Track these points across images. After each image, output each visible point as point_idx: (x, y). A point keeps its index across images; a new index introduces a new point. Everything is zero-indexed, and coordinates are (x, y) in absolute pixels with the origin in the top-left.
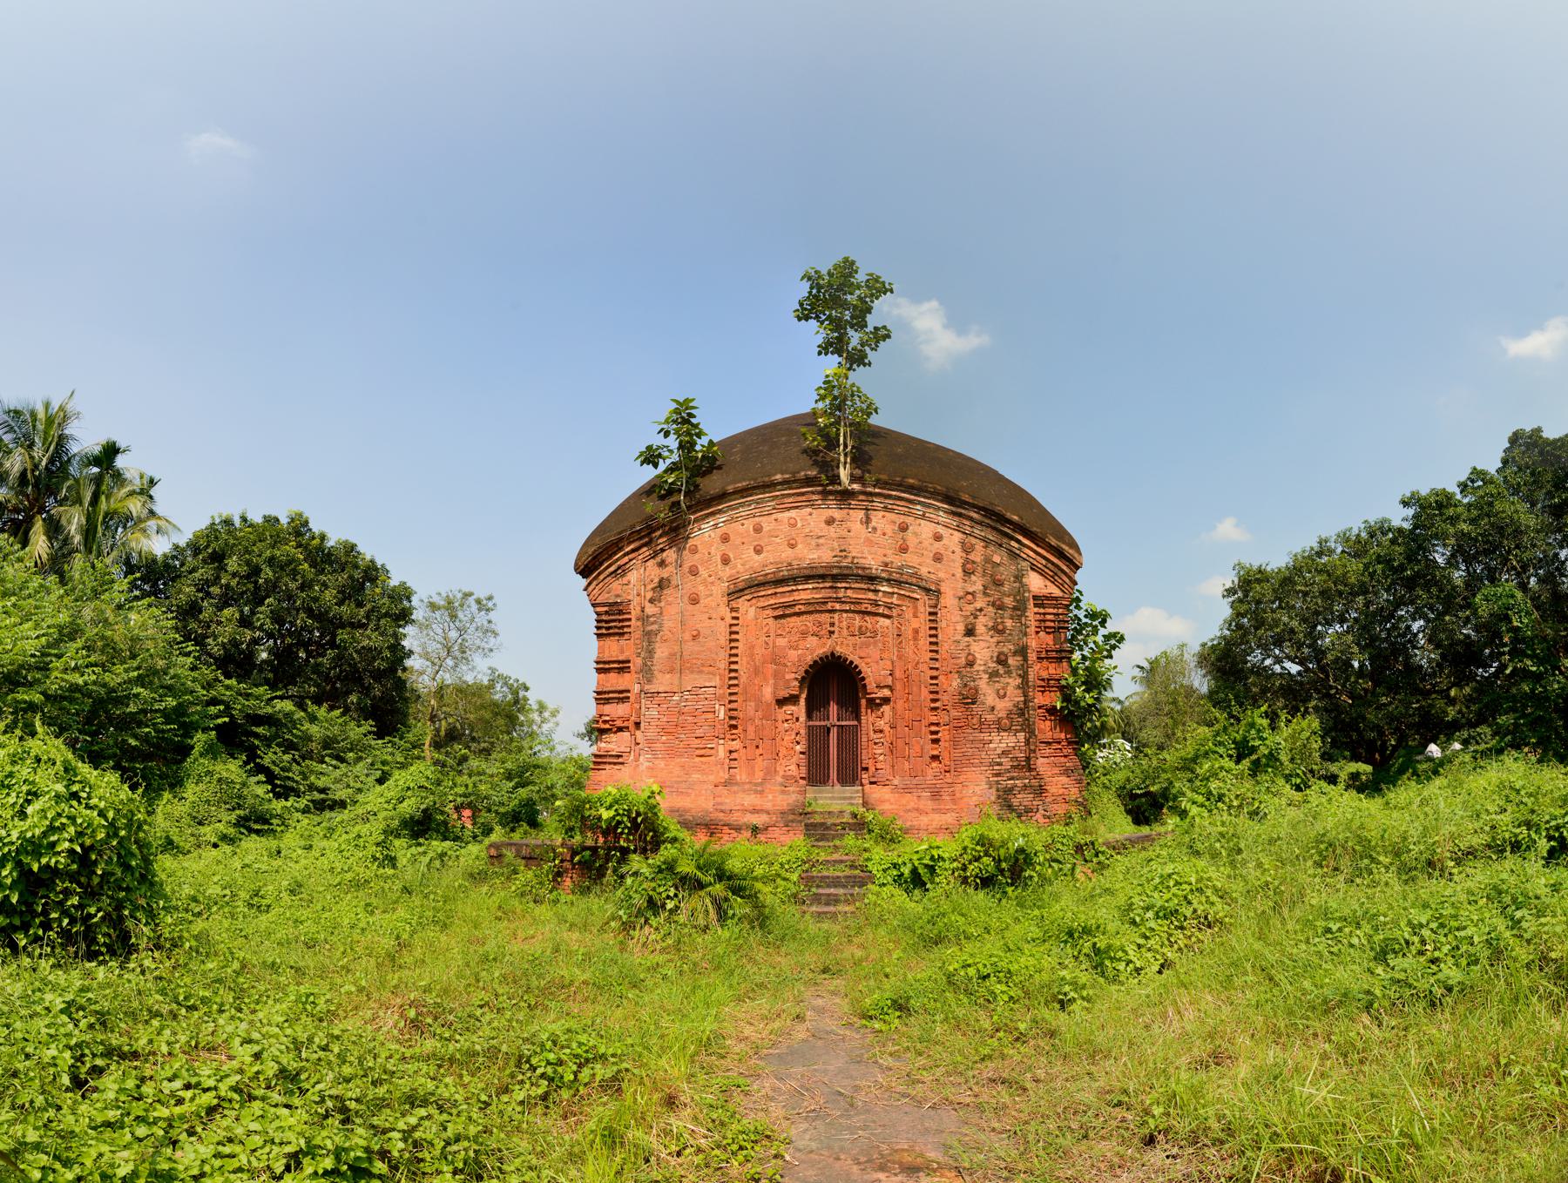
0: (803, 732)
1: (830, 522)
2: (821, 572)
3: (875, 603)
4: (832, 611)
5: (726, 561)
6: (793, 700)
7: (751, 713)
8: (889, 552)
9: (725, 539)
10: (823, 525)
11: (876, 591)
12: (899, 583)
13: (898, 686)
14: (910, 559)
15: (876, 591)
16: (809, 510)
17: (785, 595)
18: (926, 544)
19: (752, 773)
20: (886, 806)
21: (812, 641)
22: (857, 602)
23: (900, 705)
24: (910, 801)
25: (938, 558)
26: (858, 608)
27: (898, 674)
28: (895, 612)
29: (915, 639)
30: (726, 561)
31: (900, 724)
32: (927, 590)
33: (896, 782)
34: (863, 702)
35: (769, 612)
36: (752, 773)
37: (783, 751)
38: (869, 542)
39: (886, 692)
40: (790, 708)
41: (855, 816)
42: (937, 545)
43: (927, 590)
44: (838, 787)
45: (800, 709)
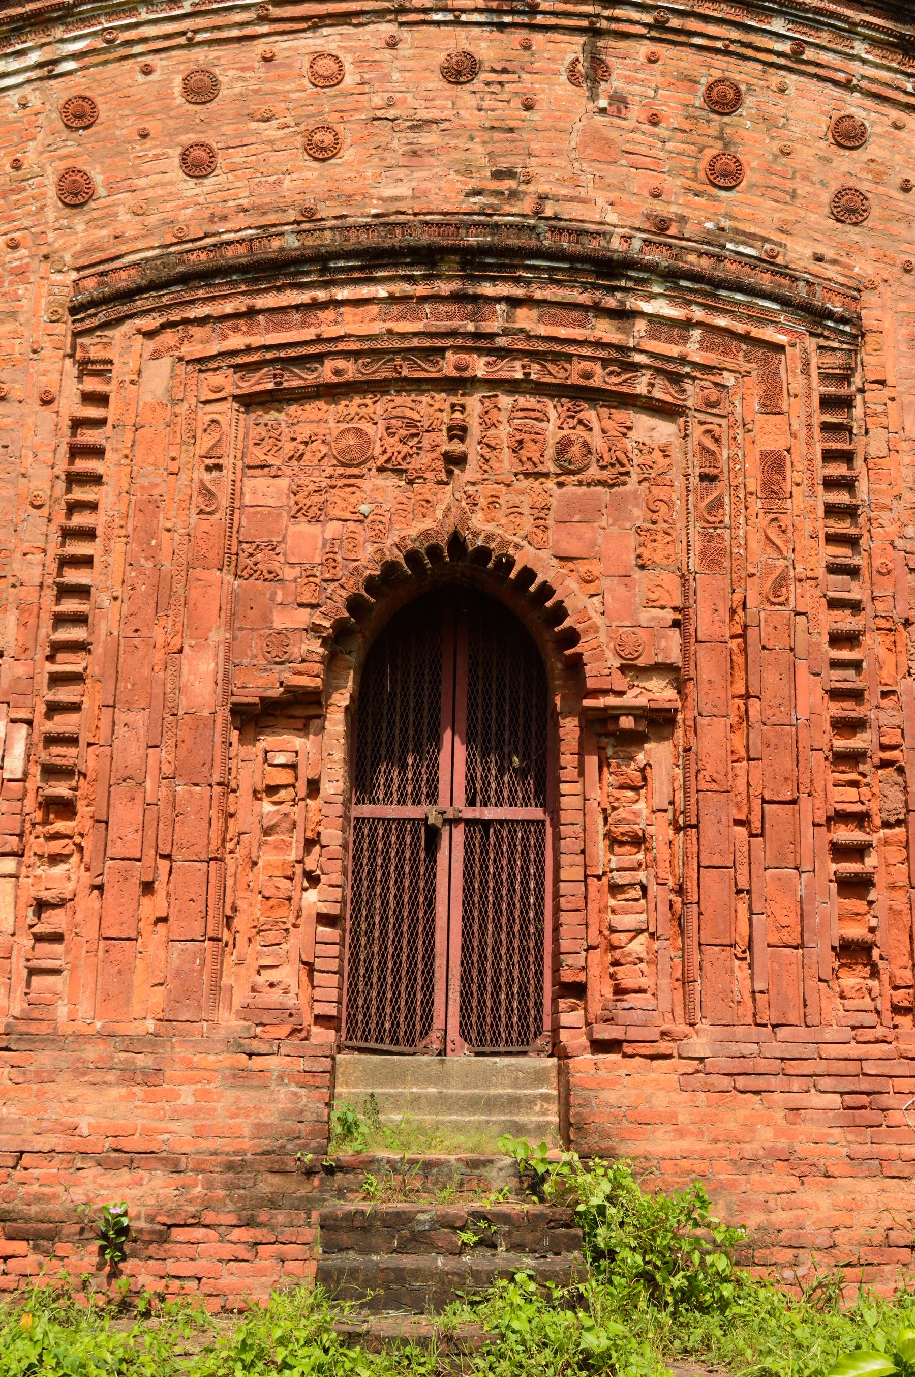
0: (332, 836)
1: (461, 71)
2: (424, 238)
3: (620, 359)
4: (459, 384)
5: (76, 194)
6: (295, 709)
7: (130, 749)
8: (673, 184)
9: (80, 115)
10: (435, 82)
11: (623, 315)
12: (709, 287)
13: (708, 667)
14: (750, 210)
15: (623, 315)
16: (387, 29)
17: (284, 321)
18: (804, 155)
19: (115, 996)
20: (660, 1143)
21: (379, 491)
22: (553, 353)
23: (714, 739)
24: (760, 1124)
25: (849, 208)
26: (556, 374)
27: (708, 621)
28: (693, 394)
29: (773, 491)
30: (76, 194)
31: (716, 815)
32: (815, 316)
33: (699, 1045)
34: (569, 728)
35: (227, 381)
36: (115, 996)
37: (251, 910)
38: (602, 148)
39: (658, 692)
40: (285, 744)
41: (531, 1181)
42: (847, 163)
43: (815, 316)
44: (462, 1058)
45: (325, 750)
